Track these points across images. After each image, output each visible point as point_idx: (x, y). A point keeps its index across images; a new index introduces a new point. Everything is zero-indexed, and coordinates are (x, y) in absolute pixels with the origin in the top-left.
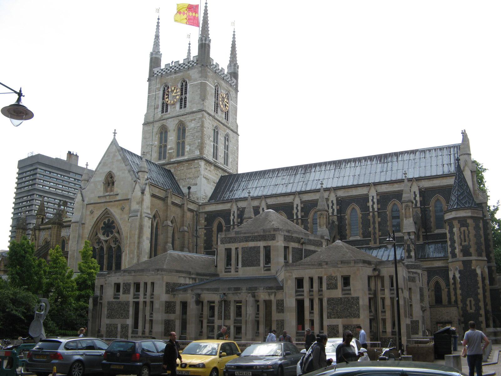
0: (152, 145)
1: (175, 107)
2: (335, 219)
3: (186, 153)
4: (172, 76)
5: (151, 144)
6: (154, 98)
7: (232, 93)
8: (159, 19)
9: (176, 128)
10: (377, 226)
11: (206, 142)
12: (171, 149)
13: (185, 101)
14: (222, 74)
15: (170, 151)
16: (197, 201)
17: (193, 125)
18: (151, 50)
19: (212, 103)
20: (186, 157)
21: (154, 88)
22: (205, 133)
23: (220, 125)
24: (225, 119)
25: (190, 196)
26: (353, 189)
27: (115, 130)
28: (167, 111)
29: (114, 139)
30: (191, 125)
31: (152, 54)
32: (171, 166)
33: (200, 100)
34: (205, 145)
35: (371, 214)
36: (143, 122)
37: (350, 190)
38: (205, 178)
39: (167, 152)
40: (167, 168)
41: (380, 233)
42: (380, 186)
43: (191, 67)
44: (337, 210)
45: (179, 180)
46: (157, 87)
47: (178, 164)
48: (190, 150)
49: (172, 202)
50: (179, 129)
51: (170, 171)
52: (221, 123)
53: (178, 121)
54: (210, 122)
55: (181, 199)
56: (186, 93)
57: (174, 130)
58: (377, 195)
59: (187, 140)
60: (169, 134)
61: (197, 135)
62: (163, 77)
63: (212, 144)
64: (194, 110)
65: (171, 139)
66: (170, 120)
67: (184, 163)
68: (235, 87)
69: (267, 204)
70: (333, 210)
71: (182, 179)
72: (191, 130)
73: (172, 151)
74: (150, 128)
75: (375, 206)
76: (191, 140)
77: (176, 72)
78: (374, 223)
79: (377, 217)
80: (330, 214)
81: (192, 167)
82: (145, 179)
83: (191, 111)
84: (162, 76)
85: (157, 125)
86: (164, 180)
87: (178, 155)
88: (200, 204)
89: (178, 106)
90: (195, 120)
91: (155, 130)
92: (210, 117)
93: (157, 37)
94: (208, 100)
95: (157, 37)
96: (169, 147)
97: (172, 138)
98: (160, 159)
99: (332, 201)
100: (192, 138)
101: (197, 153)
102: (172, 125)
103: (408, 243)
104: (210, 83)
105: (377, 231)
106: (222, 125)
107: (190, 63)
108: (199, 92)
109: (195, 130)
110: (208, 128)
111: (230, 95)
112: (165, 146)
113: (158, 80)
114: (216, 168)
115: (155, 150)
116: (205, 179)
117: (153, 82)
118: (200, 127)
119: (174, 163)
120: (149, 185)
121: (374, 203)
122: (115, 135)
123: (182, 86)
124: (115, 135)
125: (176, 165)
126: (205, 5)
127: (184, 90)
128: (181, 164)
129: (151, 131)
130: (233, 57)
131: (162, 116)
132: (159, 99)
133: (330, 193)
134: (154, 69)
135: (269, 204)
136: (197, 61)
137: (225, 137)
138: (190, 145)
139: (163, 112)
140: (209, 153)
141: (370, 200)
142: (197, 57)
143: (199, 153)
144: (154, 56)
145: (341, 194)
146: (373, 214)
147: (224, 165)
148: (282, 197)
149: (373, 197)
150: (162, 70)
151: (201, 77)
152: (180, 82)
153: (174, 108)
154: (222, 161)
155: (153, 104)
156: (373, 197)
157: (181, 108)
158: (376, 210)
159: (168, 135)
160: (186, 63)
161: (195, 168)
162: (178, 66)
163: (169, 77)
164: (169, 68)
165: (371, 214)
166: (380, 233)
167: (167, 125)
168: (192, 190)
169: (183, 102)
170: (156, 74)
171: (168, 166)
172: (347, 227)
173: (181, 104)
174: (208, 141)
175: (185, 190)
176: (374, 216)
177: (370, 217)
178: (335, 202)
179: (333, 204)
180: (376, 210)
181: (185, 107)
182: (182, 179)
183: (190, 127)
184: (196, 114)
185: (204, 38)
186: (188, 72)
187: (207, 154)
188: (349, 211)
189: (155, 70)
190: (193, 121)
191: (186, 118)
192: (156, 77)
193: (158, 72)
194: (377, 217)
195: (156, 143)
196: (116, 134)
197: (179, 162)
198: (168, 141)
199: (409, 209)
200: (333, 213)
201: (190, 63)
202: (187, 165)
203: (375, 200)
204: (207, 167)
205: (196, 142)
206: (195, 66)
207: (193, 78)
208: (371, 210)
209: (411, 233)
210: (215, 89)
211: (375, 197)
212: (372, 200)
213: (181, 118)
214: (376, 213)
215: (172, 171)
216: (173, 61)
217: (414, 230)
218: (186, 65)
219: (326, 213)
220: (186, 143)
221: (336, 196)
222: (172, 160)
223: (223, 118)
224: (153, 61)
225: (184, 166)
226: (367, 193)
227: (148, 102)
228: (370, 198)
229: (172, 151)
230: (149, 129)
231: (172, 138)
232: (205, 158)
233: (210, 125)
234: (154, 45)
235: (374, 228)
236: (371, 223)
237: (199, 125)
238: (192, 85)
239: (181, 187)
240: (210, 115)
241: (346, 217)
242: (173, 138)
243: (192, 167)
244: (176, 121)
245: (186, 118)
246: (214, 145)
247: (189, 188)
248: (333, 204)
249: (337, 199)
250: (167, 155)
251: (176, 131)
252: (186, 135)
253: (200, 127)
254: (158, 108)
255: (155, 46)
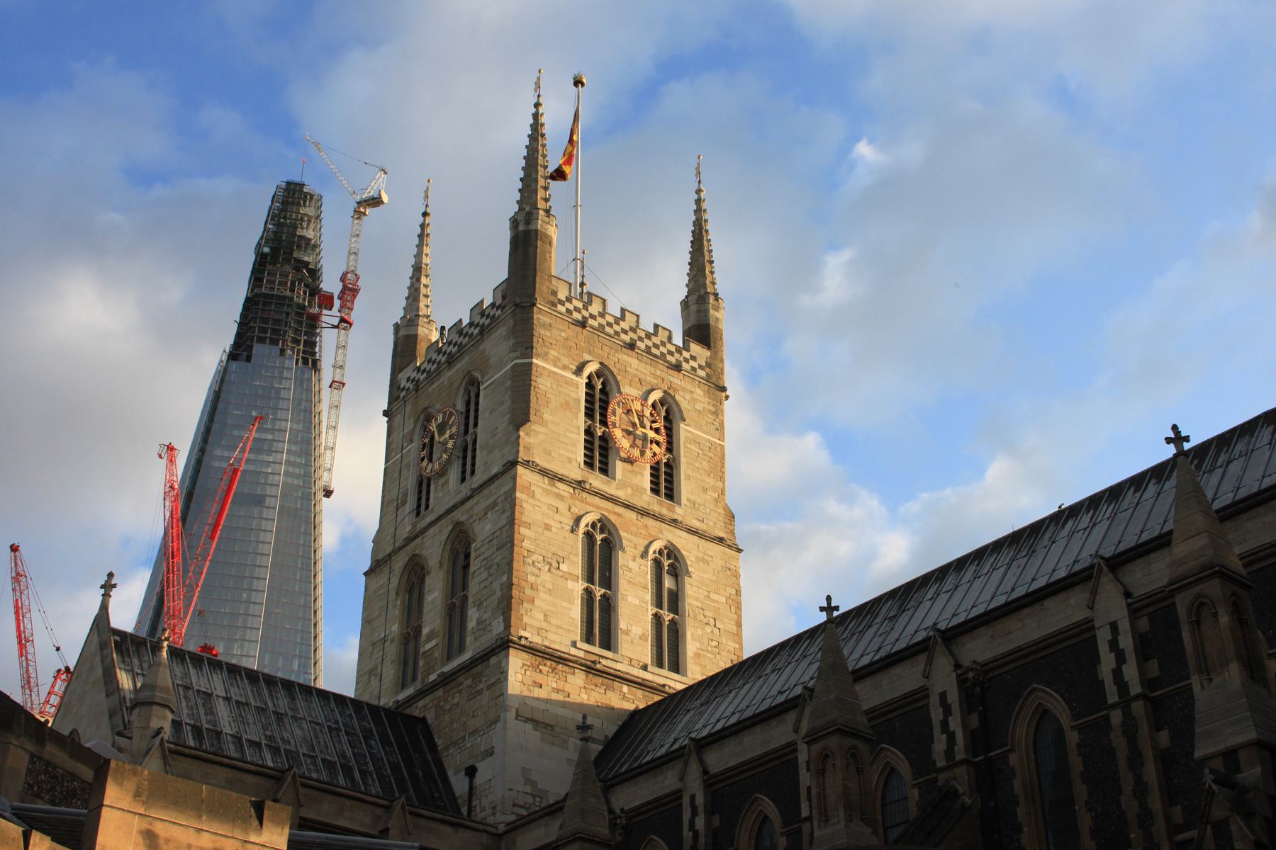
0: (384, 640)
1: (447, 482)
2: (961, 779)
3: (469, 639)
4: (442, 379)
5: (383, 636)
6: (397, 475)
7: (691, 397)
8: (425, 214)
9: (447, 553)
10: (1151, 772)
11: (531, 578)
12: (431, 636)
13: (474, 450)
14: (625, 332)
15: (428, 646)
16: (491, 820)
17: (488, 527)
18: (397, 315)
19: (574, 436)
20: (467, 656)
21: (398, 437)
22: (532, 548)
23: (618, 515)
24: (655, 490)
25: (474, 804)
26: (1026, 611)
27: (111, 575)
28: (427, 507)
29: (104, 608)
30: (483, 530)
31: (397, 327)
32: (428, 699)
33: (511, 427)
34: (528, 591)
35: (1116, 717)
36: (366, 565)
37: (1011, 623)
38: (527, 720)
39: (422, 650)
40: (417, 713)
41: (1177, 810)
42: (1140, 563)
43: (489, 325)
44: (971, 735)
45: (447, 749)
46: (406, 431)
47: (447, 688)
48: (479, 622)
49: (301, 818)
50: (454, 555)
51: (424, 720)
52: (628, 506)
53: (451, 527)
54: (562, 507)
55: (379, 811)
56: (476, 425)
57: (441, 564)
58: (1134, 612)
59: (474, 587)
60: (428, 581)
61: (497, 560)
62: (420, 392)
63: (578, 587)
64: (495, 470)
65: (433, 601)
66: (431, 531)
67: (461, 679)
68: (702, 373)
69: (705, 772)
70: (951, 737)
71: (455, 744)
72: (483, 549)
73: (433, 643)
74: (382, 579)
75: (1131, 671)
76: (482, 585)
77: (451, 360)
78: (1135, 760)
79: (1144, 728)
80: (941, 763)
81: (481, 686)
82: (150, 733)
83: (485, 478)
84: (417, 391)
85: (399, 563)
86: (349, 753)
87: (449, 658)
88: (502, 828)
89: (454, 473)
90: (495, 504)
91: (395, 582)
92: (559, 485)
93: (418, 270)
94: (543, 423)
95: (418, 270)
96: (425, 631)
97: (435, 594)
98: (404, 686)
99: (943, 696)
100: (485, 575)
101: (498, 627)
102: (434, 548)
103: (1218, 813)
104: (555, 366)
105: (1155, 802)
106: (631, 515)
107: (487, 313)
108: (508, 404)
109: (494, 541)
110: (548, 527)
111: (674, 406)
112: (418, 630)
113: (408, 408)
114: (600, 680)
115: (392, 650)
116: (529, 726)
117: (398, 419)
118: (507, 527)
119: (433, 687)
120: (164, 758)
121: (1121, 658)
122: (106, 596)
123: (468, 403)
124: (106, 596)
125: (440, 693)
126: (534, 110)
127: (470, 416)
128: (454, 683)
129: (382, 592)
130: (695, 276)
131: (414, 526)
132: (409, 471)
133: (930, 662)
134: (400, 376)
135: (714, 770)
136: (504, 297)
137: (657, 564)
138: (479, 605)
139: (418, 514)
140: (554, 621)
141: (1103, 648)
142: (504, 284)
143: (501, 628)
144: (402, 332)
145: (978, 650)
146: (1127, 714)
147: (657, 670)
148: (757, 729)
149: (1114, 627)
150: (418, 369)
151: (513, 350)
152: (462, 390)
153: (443, 485)
154: (646, 655)
155: (394, 493)
156: (1114, 627)
157: (463, 480)
158: (1135, 689)
159: (427, 588)
160: (477, 319)
161: (489, 687)
162: (455, 338)
163: (434, 386)
164: (434, 356)
165: (1116, 717)
166: (1177, 810)
167: (425, 553)
168: (480, 779)
169: (467, 453)
170: (404, 388)
171: (421, 704)
172: (1021, 812)
173: (464, 465)
174: (546, 578)
175: (459, 784)
176: (1130, 728)
177: (1118, 741)
178: (953, 698)
179: (947, 710)
180: (1135, 689)
181: (473, 472)
182: (455, 744)
183: (480, 538)
184: (497, 483)
185: (520, 218)
186: (481, 347)
187: (544, 625)
188: (1021, 730)
189: (402, 376)
190: (489, 514)
191: (472, 508)
192: (404, 397)
193: (408, 379)
194: (1144, 728)
195: (395, 628)
196: (114, 592)
197: (447, 680)
198: (426, 609)
199: (1215, 615)
200: (949, 753)
201: (487, 313)
202: (468, 682)
203: (1126, 642)
204: (539, 678)
205: (496, 585)
206: (499, 317)
207: (492, 360)
208: (1112, 696)
209: (1242, 755)
210: (589, 385)
211: (1124, 625)
212: (1114, 645)
213: (459, 515)
214: (1138, 708)
215: (430, 717)
216: (443, 328)
217: (1252, 735)
218: (477, 325)
219: (848, 742)
220: (470, 600)
221: (957, 666)
222: (433, 677)
223: (638, 490)
224: (399, 349)
225: (460, 692)
226: (1079, 615)
227: (383, 491)
228: (1103, 636)
229: (433, 643)
230: (381, 583)
231: (435, 594)
232: (523, 642)
233: (557, 517)
234: (407, 298)
235: (1141, 790)
236: (1122, 763)
237: (504, 520)
238: (491, 388)
239: (450, 773)
240: (555, 477)
241: (1013, 759)
242: (436, 594)
243: (481, 686)
244: (445, 528)
245: (472, 508)
246: (589, 594)
247: (471, 772)
248: (947, 710)
249: (962, 681)
250: (421, 663)
251: (445, 567)
252: (472, 569)
253: (507, 527)
254: (404, 503)
255: (410, 300)
